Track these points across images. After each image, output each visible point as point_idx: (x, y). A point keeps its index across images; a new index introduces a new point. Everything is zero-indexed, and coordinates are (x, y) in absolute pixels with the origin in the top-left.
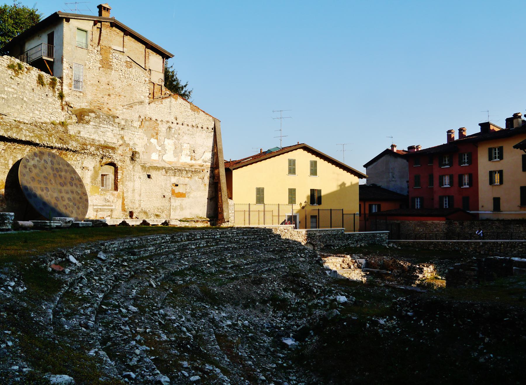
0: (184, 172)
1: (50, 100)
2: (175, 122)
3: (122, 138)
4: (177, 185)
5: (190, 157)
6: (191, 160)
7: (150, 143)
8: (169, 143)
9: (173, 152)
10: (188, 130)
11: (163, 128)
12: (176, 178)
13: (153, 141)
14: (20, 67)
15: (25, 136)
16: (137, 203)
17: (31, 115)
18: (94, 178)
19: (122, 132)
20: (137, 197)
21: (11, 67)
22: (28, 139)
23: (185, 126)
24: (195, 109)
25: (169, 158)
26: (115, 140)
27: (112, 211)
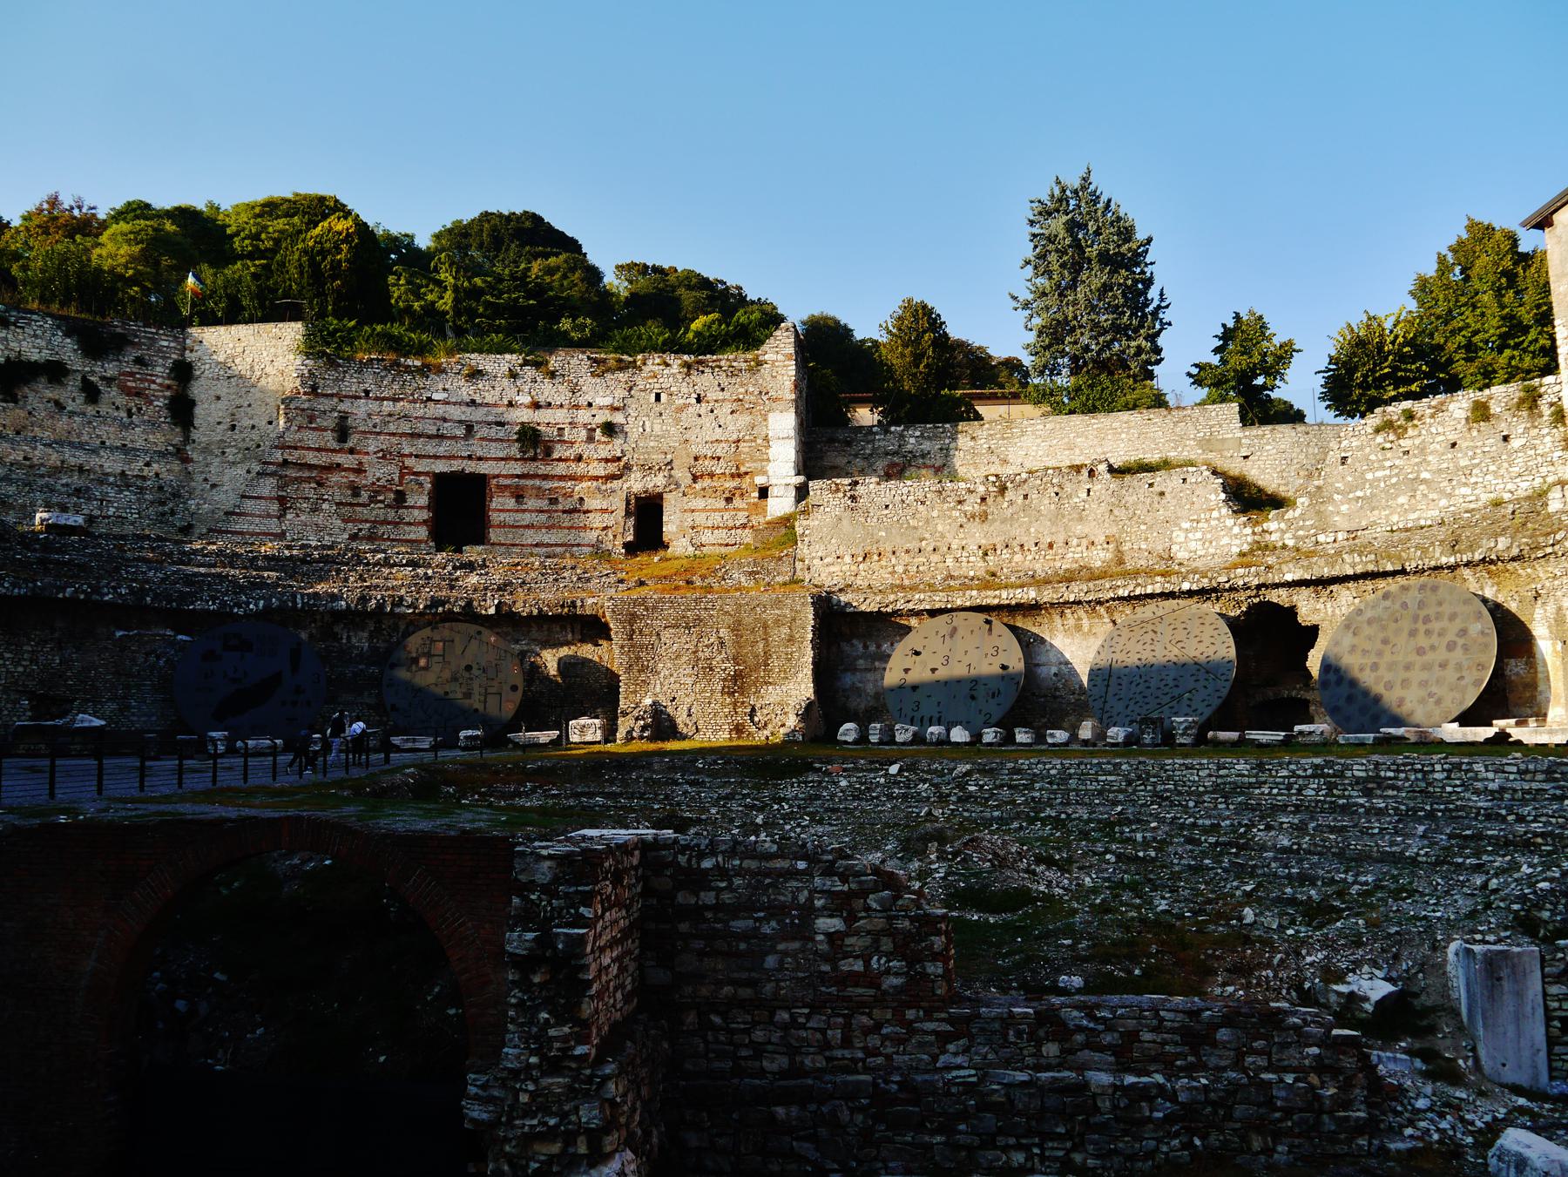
1: (1515, 443)
14: (1410, 416)
15: (1353, 565)
17: (1443, 502)
21: (1388, 426)
22: (1359, 569)
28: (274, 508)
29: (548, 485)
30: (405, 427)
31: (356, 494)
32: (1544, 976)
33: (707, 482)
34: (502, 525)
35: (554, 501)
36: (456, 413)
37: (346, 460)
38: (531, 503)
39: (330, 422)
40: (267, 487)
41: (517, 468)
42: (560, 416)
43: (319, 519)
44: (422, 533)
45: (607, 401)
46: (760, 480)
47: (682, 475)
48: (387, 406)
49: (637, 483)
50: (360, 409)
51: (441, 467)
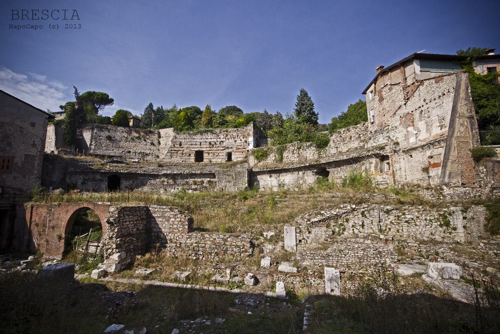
0: (437, 144)
2: (424, 104)
3: (389, 137)
4: (432, 157)
5: (440, 128)
6: (441, 129)
7: (408, 131)
9: (425, 130)
10: (436, 103)
11: (417, 115)
12: (431, 151)
13: (410, 129)
16: (404, 177)
18: (376, 167)
20: (403, 173)
23: (433, 102)
25: (424, 136)
26: (385, 141)
28: (170, 157)
29: (214, 151)
30: (190, 143)
31: (183, 154)
32: (296, 232)
33: (239, 150)
34: (206, 158)
35: (214, 154)
36: (198, 140)
37: (181, 149)
38: (210, 155)
39: (178, 143)
40: (169, 154)
41: (208, 149)
42: (215, 140)
43: (177, 159)
44: (193, 160)
45: (223, 137)
46: (247, 149)
47: (234, 149)
48: (188, 140)
49: (230, 150)
50: (183, 141)
51: (196, 149)
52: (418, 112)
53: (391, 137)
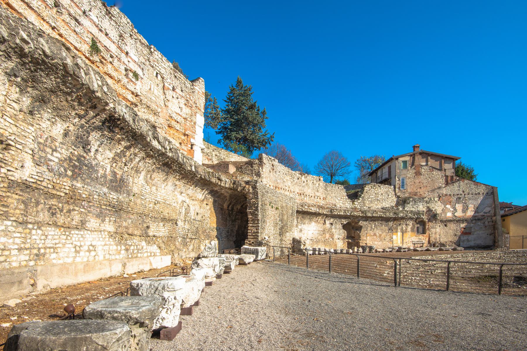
8: (459, 207)
13: (448, 206)
19: (428, 205)
20: (438, 236)
24: (477, 184)
25: (459, 214)
27: (423, 244)
52: (456, 197)
53: (431, 207)
